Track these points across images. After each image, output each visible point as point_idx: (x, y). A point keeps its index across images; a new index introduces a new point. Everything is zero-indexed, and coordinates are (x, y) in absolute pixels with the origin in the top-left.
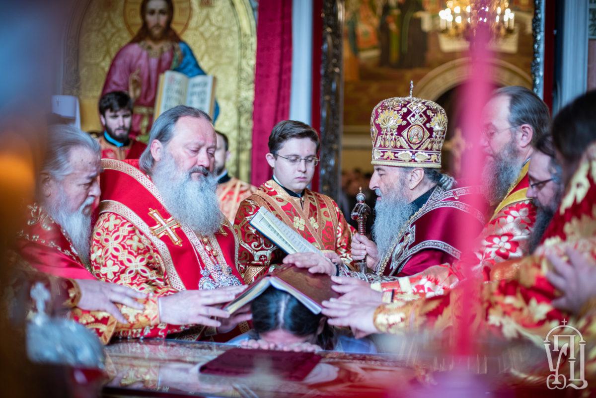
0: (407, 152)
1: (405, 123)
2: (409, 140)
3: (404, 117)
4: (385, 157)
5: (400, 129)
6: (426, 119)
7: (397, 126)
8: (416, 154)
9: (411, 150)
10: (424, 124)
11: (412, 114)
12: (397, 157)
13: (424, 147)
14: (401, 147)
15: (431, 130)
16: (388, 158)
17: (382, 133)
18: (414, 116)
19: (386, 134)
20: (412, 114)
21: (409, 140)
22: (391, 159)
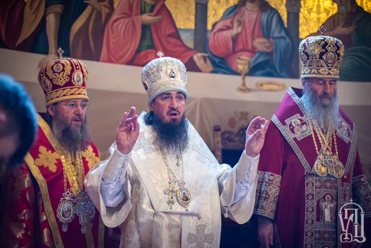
0: (325, 69)
1: (324, 50)
2: (326, 61)
3: (324, 47)
4: (312, 73)
5: (321, 55)
6: (337, 48)
7: (319, 53)
8: (331, 70)
9: (328, 68)
10: (336, 52)
11: (328, 45)
12: (319, 72)
13: (335, 65)
14: (322, 66)
15: (339, 55)
16: (314, 73)
17: (310, 57)
18: (330, 46)
19: (312, 59)
20: (328, 45)
21: (326, 61)
22: (316, 74)
